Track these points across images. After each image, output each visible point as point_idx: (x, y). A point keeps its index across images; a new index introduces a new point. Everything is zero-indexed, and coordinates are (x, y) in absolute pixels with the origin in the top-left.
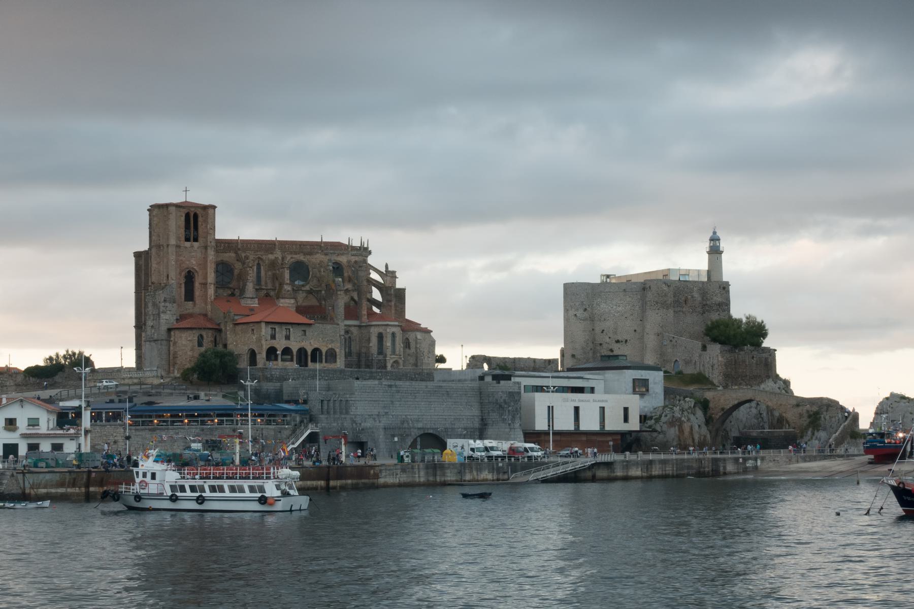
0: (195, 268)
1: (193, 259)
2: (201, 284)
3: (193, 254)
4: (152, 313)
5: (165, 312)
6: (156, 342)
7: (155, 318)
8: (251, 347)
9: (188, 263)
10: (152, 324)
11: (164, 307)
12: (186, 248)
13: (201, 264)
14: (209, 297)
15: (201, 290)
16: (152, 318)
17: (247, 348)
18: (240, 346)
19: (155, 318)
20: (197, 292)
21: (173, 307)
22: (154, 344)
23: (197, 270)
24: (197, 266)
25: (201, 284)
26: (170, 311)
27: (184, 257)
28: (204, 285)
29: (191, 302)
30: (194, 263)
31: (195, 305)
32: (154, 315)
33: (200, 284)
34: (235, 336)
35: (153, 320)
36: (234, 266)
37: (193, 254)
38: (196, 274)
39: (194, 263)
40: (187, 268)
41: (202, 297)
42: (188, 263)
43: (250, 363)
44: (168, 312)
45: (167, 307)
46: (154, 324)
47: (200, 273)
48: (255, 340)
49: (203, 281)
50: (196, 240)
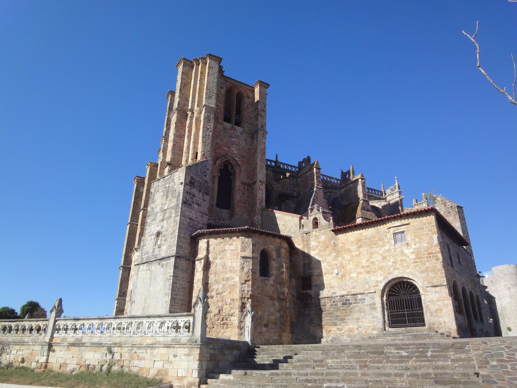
0: (236, 159)
1: (234, 146)
2: (243, 183)
3: (234, 139)
4: (161, 208)
5: (190, 205)
6: (164, 262)
7: (167, 215)
8: (397, 274)
9: (226, 149)
10: (158, 229)
11: (190, 194)
12: (225, 128)
13: (245, 157)
14: (258, 201)
15: (244, 194)
16: (160, 217)
17: (381, 278)
18: (354, 275)
19: (167, 215)
20: (238, 196)
21: (204, 200)
22: (158, 267)
23: (238, 162)
24: (239, 158)
25: (243, 183)
26: (199, 205)
27: (222, 140)
28: (250, 186)
29: (226, 211)
30: (235, 152)
31: (232, 215)
32: (164, 211)
33: (242, 183)
34: (336, 258)
35: (163, 220)
36: (272, 187)
37: (234, 139)
38: (238, 167)
39: (235, 152)
40: (225, 156)
41: (244, 203)
42: (226, 149)
43: (391, 316)
44: (196, 206)
45: (194, 196)
46: (162, 227)
47: (243, 169)
48: (413, 256)
49: (247, 181)
50: (238, 123)
